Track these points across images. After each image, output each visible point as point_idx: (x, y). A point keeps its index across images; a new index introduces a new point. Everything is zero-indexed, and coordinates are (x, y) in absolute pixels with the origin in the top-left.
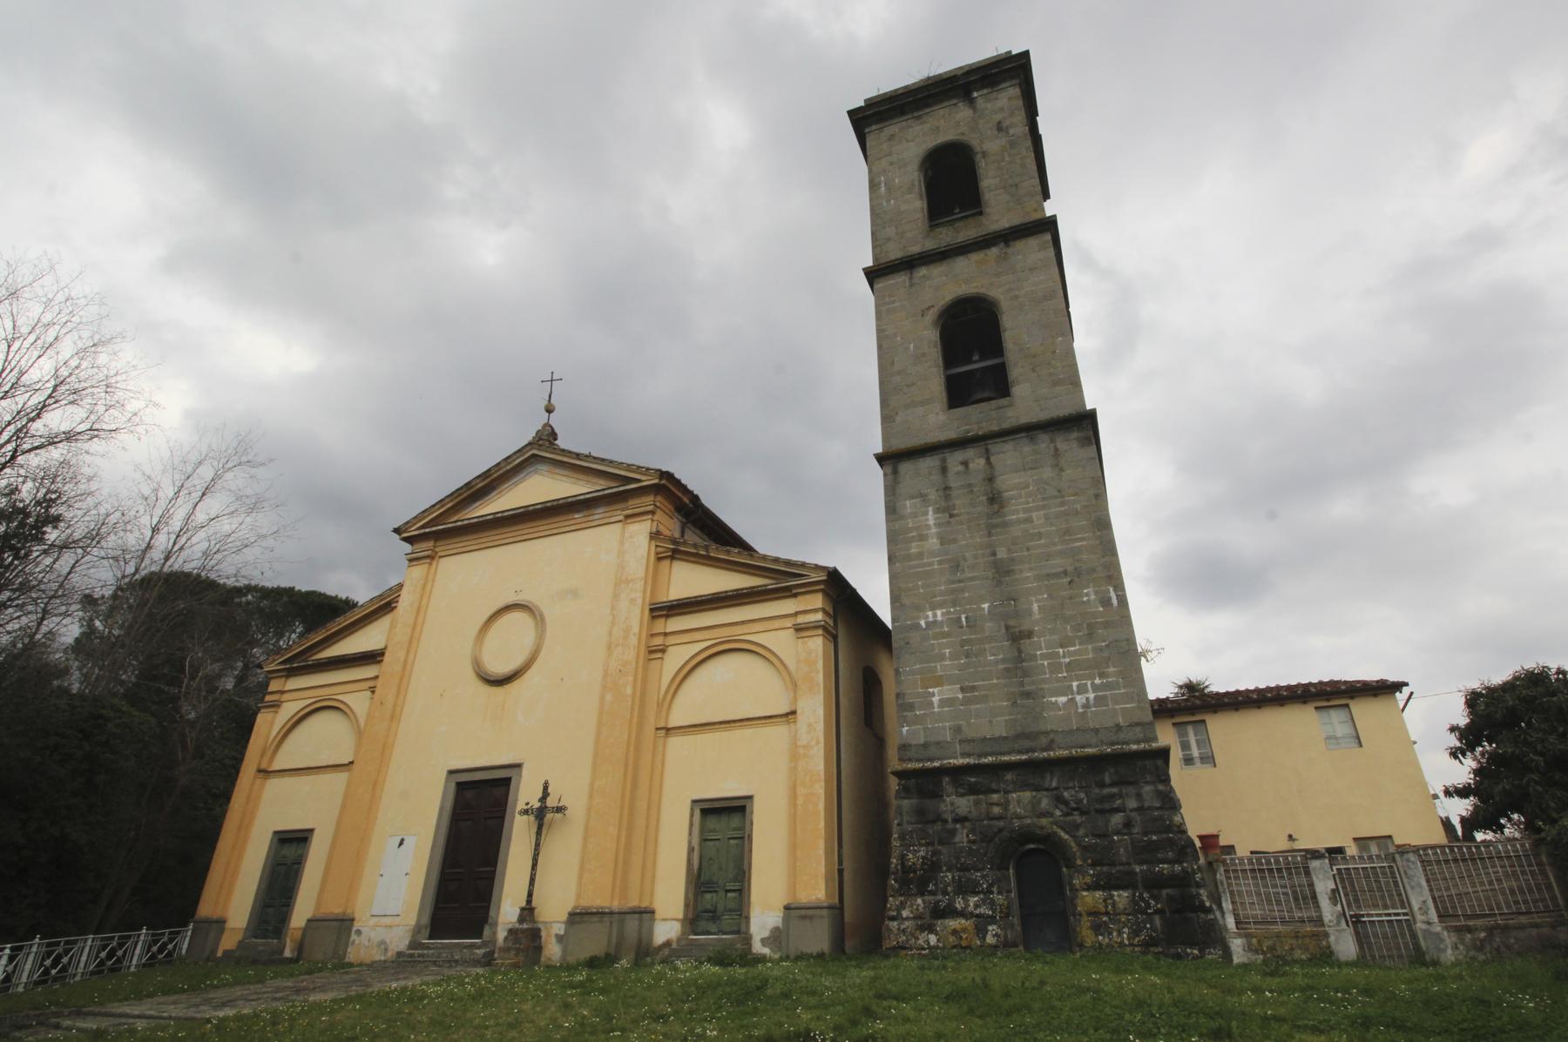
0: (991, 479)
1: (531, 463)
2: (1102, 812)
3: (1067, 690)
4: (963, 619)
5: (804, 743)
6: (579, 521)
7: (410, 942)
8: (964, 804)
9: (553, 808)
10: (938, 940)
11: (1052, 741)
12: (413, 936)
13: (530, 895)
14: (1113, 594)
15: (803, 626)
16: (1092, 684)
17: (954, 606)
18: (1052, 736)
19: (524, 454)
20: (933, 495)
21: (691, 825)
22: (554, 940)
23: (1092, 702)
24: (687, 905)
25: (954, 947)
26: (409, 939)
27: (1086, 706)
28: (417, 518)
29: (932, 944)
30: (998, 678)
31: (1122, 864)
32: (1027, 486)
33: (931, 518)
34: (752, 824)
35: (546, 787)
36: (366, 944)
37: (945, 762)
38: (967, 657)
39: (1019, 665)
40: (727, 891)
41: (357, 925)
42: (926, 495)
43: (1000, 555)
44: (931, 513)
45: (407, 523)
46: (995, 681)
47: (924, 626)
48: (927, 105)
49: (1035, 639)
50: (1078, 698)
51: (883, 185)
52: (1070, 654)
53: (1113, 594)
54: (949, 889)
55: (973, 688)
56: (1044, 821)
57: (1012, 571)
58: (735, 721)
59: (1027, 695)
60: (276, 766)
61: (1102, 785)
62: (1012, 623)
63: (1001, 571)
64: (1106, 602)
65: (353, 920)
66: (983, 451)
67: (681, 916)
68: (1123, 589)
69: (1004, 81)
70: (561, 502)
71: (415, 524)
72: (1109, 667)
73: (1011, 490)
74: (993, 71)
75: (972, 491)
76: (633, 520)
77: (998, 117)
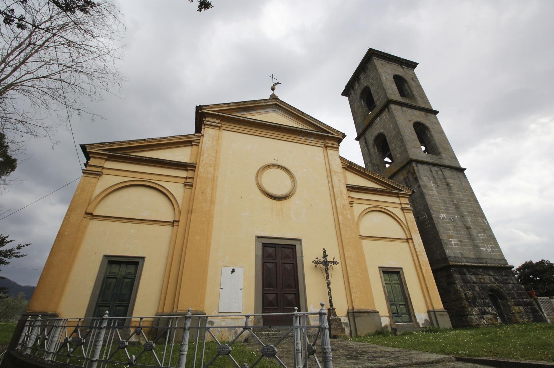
0: (445, 179)
1: (273, 107)
3: (484, 247)
9: (331, 262)
13: (331, 302)
15: (406, 208)
19: (281, 104)
20: (431, 178)
21: (381, 277)
24: (389, 310)
30: (467, 240)
33: (433, 185)
34: (405, 279)
35: (324, 252)
38: (457, 231)
39: (470, 237)
44: (432, 183)
45: (208, 106)
48: (390, 61)
49: (472, 230)
50: (488, 249)
51: (384, 76)
54: (482, 305)
56: (495, 285)
57: (459, 208)
58: (387, 238)
60: (98, 212)
61: (503, 276)
62: (465, 223)
63: (457, 207)
64: (485, 223)
67: (388, 315)
70: (298, 129)
71: (211, 108)
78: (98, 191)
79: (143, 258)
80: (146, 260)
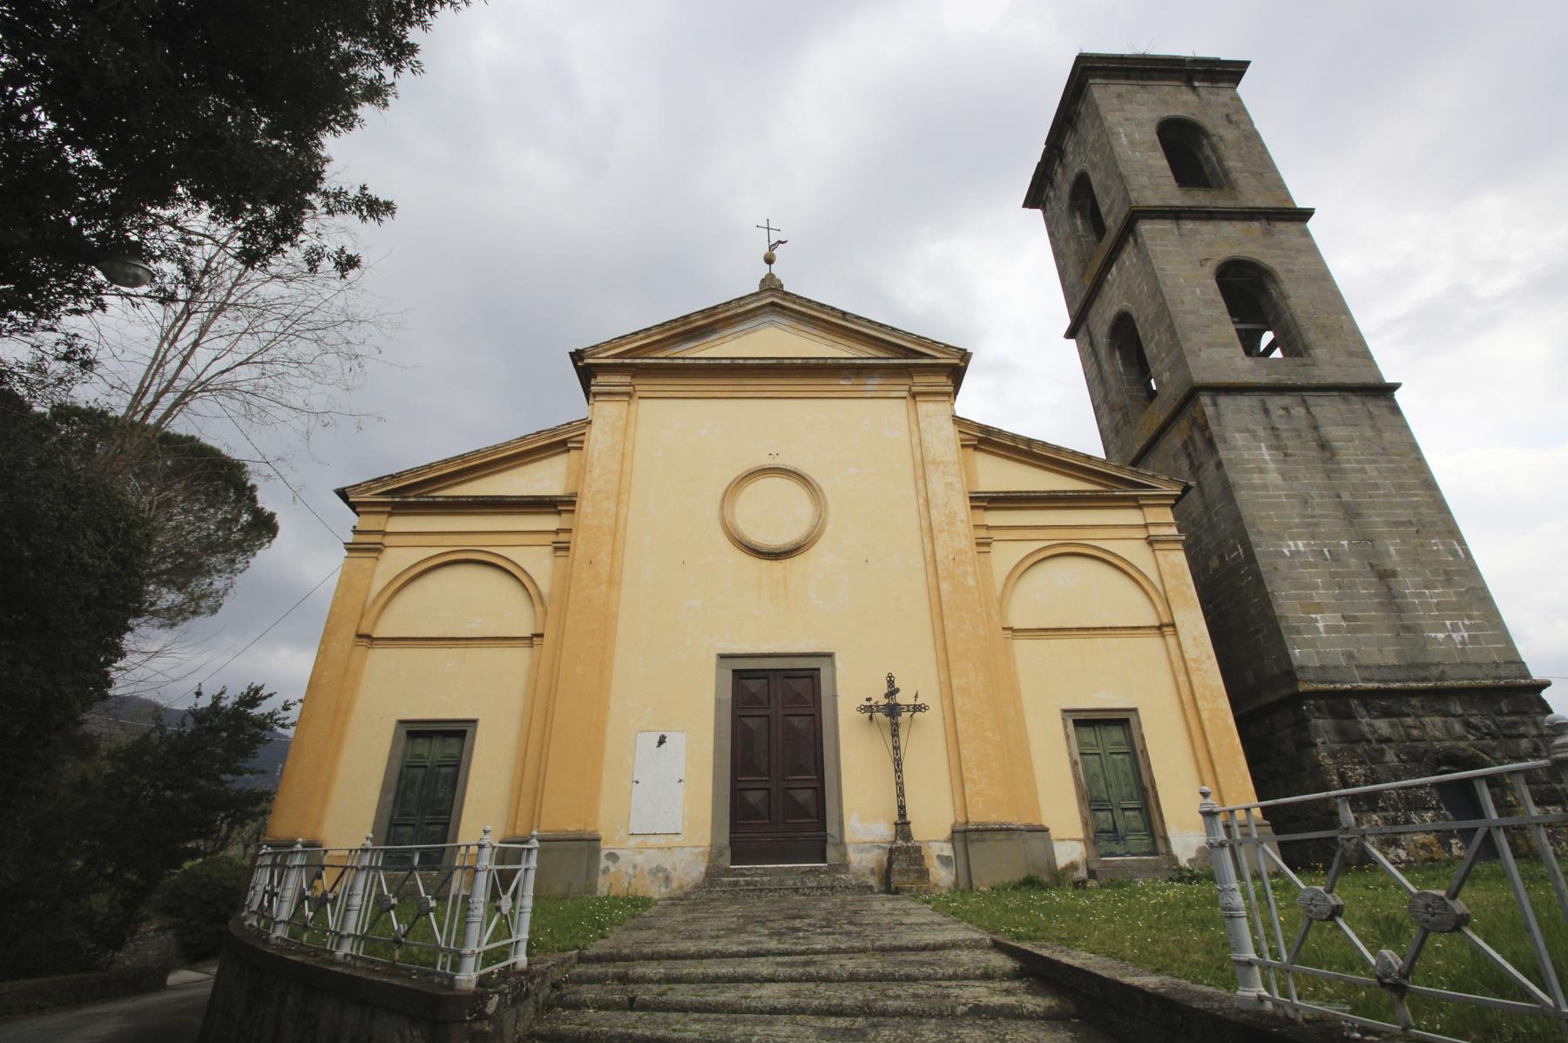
0: (1315, 428)
1: (766, 313)
2: (1510, 737)
3: (1443, 628)
4: (1326, 553)
5: (1194, 657)
6: (848, 388)
7: (708, 868)
8: (1383, 726)
9: (908, 706)
10: (1408, 854)
11: (1443, 672)
12: (711, 860)
13: (902, 807)
14: (1458, 547)
15: (1161, 538)
16: (1463, 624)
17: (1314, 539)
18: (1441, 668)
19: (784, 299)
20: (1261, 433)
21: (1067, 737)
22: (936, 863)
23: (1467, 640)
24: (1085, 824)
25: (1426, 860)
26: (706, 864)
27: (1463, 642)
28: (610, 344)
29: (1403, 858)
30: (1376, 611)
31: (1544, 783)
32: (1352, 440)
33: (1266, 454)
34: (1143, 739)
35: (891, 681)
36: (631, 871)
37: (1355, 685)
38: (1340, 588)
39: (1391, 601)
40: (1124, 810)
41: (605, 848)
42: (1254, 431)
43: (1344, 499)
44: (1264, 449)
45: (597, 346)
46: (1373, 613)
47: (1288, 554)
48: (1151, 78)
49: (1401, 579)
50: (1454, 635)
51: (1123, 135)
52: (1437, 595)
53: (1458, 547)
54: (1400, 806)
55: (1355, 618)
56: (1462, 744)
57: (1361, 514)
58: (1095, 629)
59: (1408, 629)
60: (381, 631)
61: (1501, 714)
62: (1374, 561)
63: (1351, 514)
64: (1454, 553)
65: (599, 840)
66: (1300, 400)
67: (1081, 835)
68: (1465, 545)
69: (1223, 81)
70: (829, 361)
71: (605, 351)
72: (1472, 610)
73: (1339, 441)
74: (1218, 69)
75: (1300, 436)
76: (928, 399)
77: (1226, 110)
78: (378, 585)
79: (474, 722)
80: (480, 726)
